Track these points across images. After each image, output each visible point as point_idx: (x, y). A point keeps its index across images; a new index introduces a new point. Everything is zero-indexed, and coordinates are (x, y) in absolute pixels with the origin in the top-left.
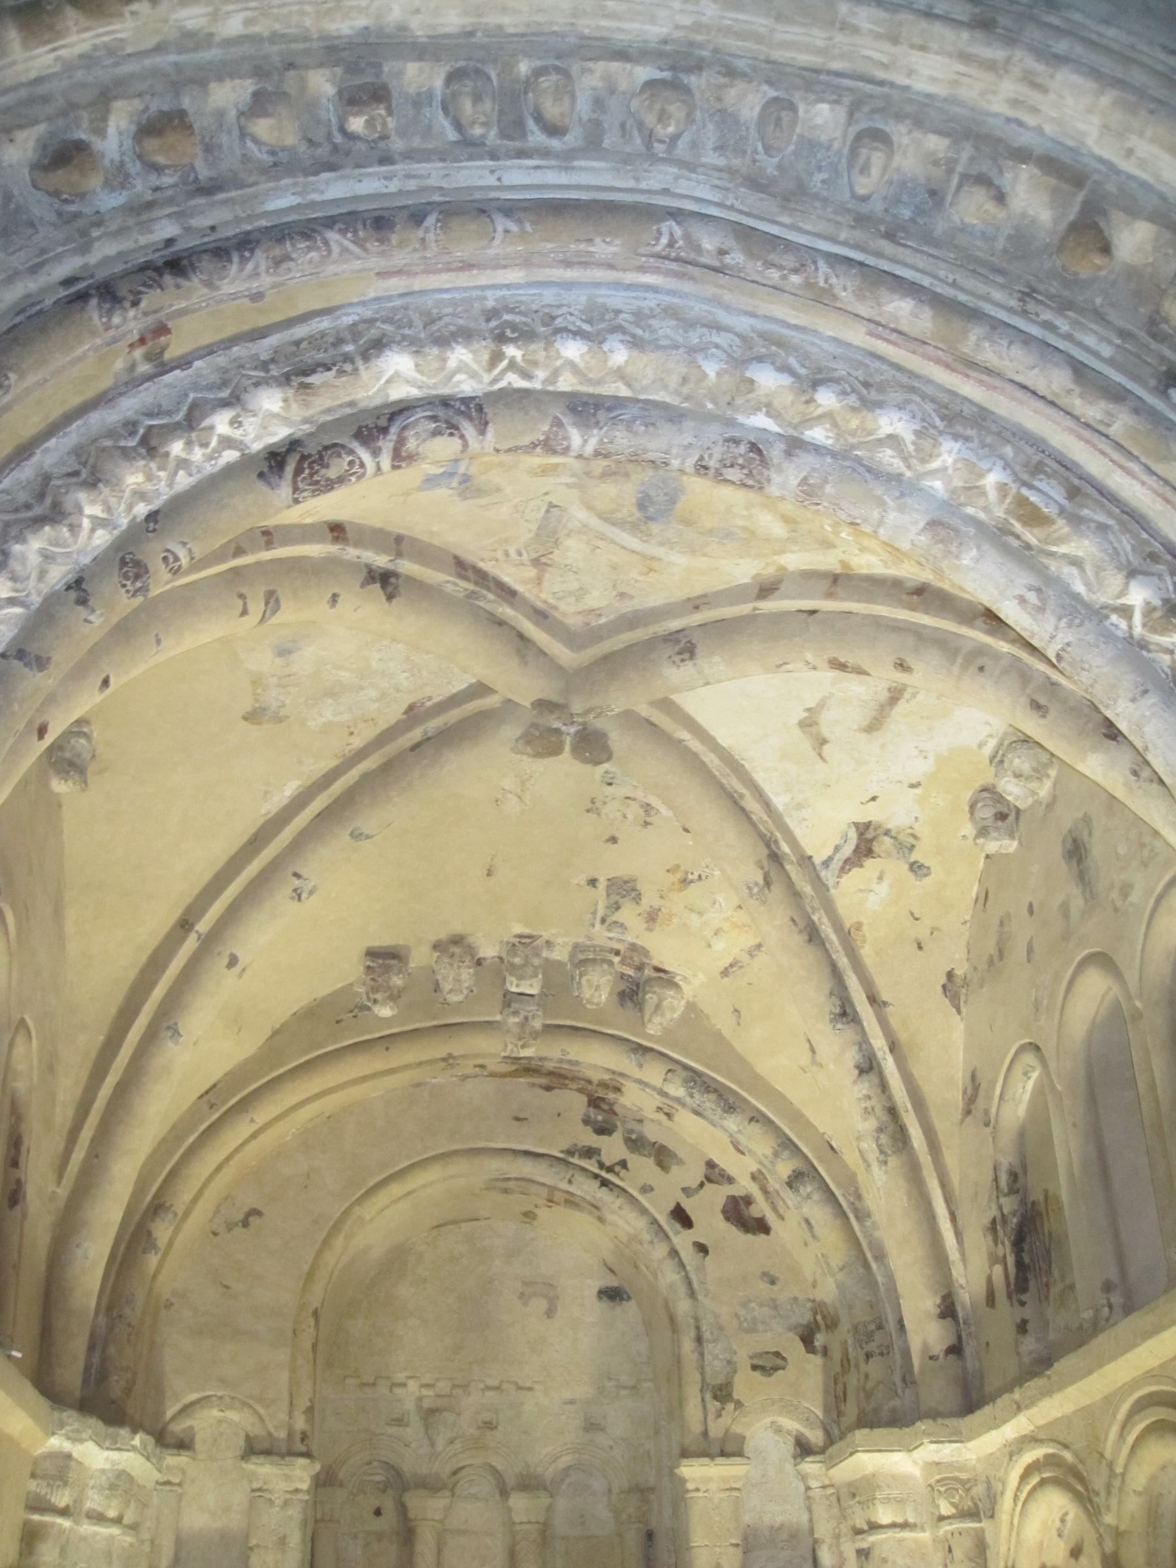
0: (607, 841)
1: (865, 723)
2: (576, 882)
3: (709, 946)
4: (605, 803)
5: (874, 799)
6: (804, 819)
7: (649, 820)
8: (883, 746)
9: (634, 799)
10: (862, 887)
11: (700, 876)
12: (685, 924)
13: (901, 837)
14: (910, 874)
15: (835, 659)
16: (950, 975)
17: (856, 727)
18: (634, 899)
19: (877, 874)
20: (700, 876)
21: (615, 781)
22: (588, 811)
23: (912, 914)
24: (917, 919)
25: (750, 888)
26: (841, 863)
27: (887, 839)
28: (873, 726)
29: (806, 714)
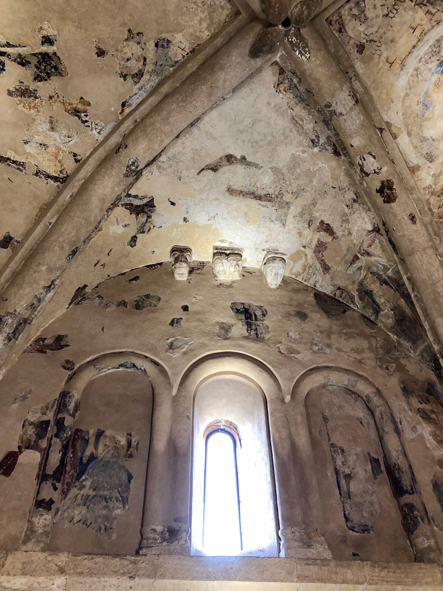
0: (98, 48)
1: (236, 187)
2: (45, 26)
3: (26, 143)
4: (139, 43)
5: (173, 204)
6: (152, 173)
7: (129, 79)
8: (217, 199)
9: (144, 64)
10: (119, 220)
11: (86, 121)
12: (34, 120)
13: (148, 224)
14: (130, 238)
15: (393, 183)
16: (85, 286)
17: (231, 183)
18: (38, 76)
19: (127, 223)
20: (86, 121)
21: (160, 49)
22: (129, 31)
23: (110, 251)
24: (108, 254)
25: (133, 164)
26: (129, 202)
27: (145, 218)
28: (231, 191)
29: (239, 157)
